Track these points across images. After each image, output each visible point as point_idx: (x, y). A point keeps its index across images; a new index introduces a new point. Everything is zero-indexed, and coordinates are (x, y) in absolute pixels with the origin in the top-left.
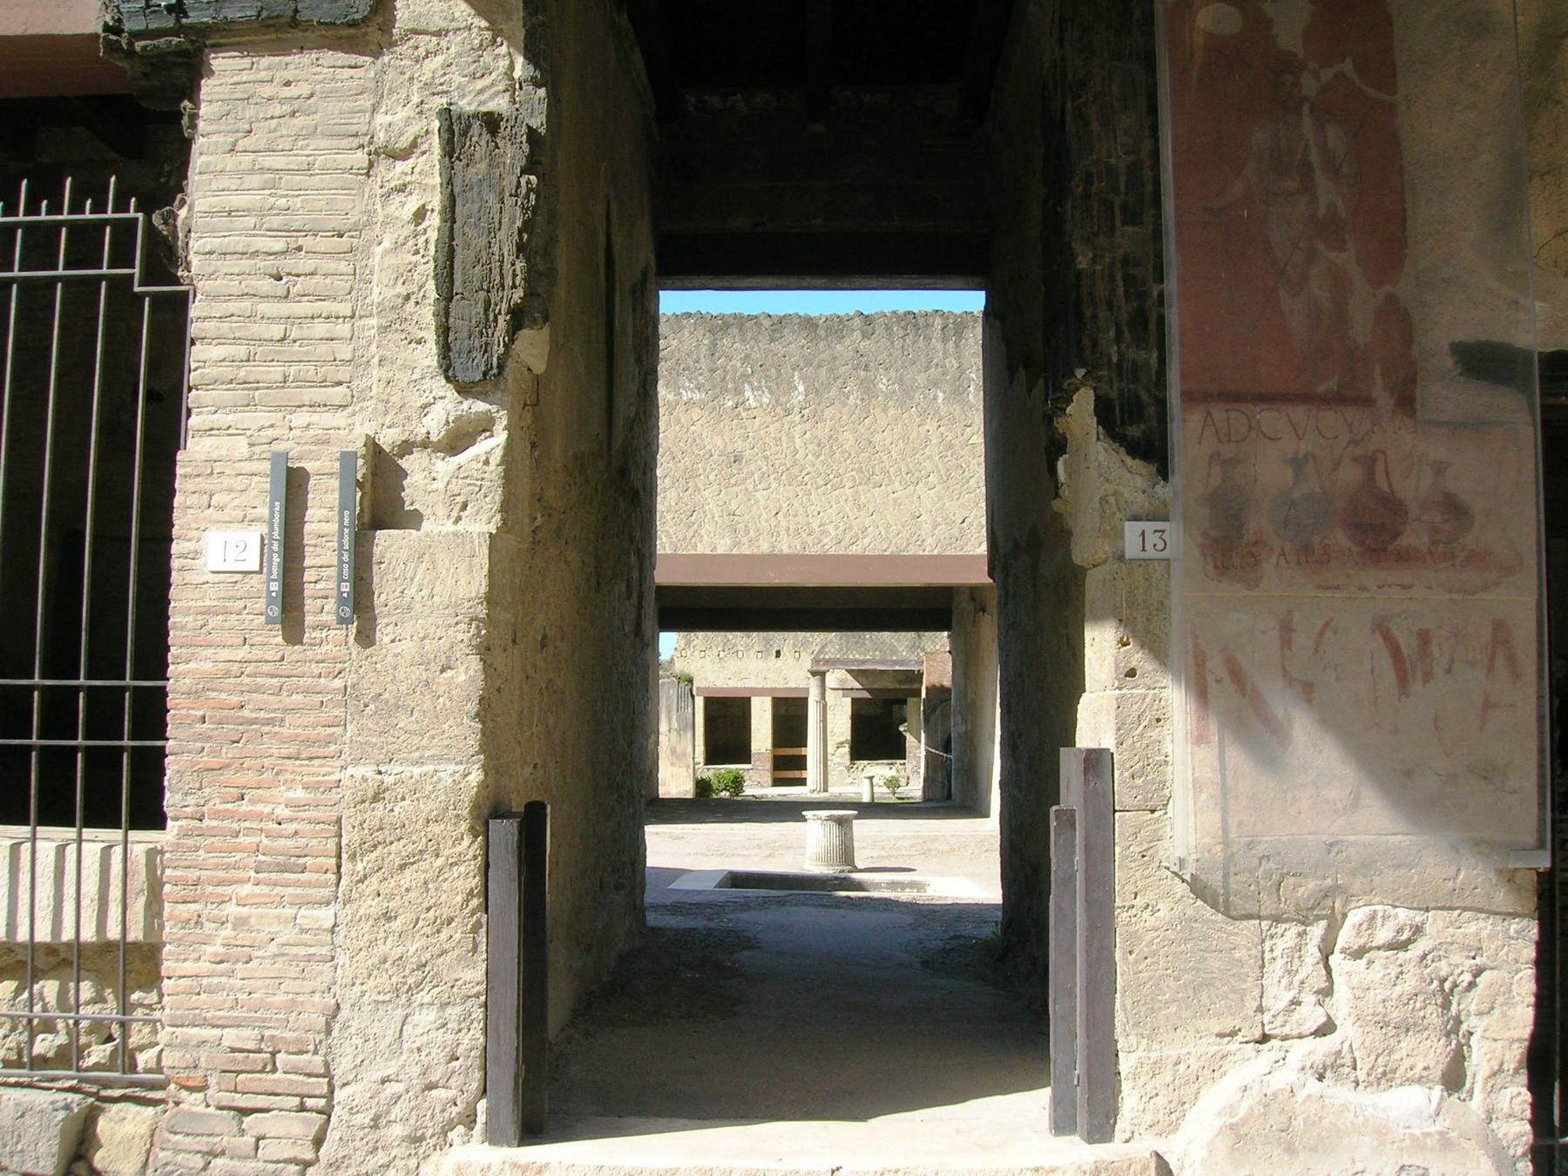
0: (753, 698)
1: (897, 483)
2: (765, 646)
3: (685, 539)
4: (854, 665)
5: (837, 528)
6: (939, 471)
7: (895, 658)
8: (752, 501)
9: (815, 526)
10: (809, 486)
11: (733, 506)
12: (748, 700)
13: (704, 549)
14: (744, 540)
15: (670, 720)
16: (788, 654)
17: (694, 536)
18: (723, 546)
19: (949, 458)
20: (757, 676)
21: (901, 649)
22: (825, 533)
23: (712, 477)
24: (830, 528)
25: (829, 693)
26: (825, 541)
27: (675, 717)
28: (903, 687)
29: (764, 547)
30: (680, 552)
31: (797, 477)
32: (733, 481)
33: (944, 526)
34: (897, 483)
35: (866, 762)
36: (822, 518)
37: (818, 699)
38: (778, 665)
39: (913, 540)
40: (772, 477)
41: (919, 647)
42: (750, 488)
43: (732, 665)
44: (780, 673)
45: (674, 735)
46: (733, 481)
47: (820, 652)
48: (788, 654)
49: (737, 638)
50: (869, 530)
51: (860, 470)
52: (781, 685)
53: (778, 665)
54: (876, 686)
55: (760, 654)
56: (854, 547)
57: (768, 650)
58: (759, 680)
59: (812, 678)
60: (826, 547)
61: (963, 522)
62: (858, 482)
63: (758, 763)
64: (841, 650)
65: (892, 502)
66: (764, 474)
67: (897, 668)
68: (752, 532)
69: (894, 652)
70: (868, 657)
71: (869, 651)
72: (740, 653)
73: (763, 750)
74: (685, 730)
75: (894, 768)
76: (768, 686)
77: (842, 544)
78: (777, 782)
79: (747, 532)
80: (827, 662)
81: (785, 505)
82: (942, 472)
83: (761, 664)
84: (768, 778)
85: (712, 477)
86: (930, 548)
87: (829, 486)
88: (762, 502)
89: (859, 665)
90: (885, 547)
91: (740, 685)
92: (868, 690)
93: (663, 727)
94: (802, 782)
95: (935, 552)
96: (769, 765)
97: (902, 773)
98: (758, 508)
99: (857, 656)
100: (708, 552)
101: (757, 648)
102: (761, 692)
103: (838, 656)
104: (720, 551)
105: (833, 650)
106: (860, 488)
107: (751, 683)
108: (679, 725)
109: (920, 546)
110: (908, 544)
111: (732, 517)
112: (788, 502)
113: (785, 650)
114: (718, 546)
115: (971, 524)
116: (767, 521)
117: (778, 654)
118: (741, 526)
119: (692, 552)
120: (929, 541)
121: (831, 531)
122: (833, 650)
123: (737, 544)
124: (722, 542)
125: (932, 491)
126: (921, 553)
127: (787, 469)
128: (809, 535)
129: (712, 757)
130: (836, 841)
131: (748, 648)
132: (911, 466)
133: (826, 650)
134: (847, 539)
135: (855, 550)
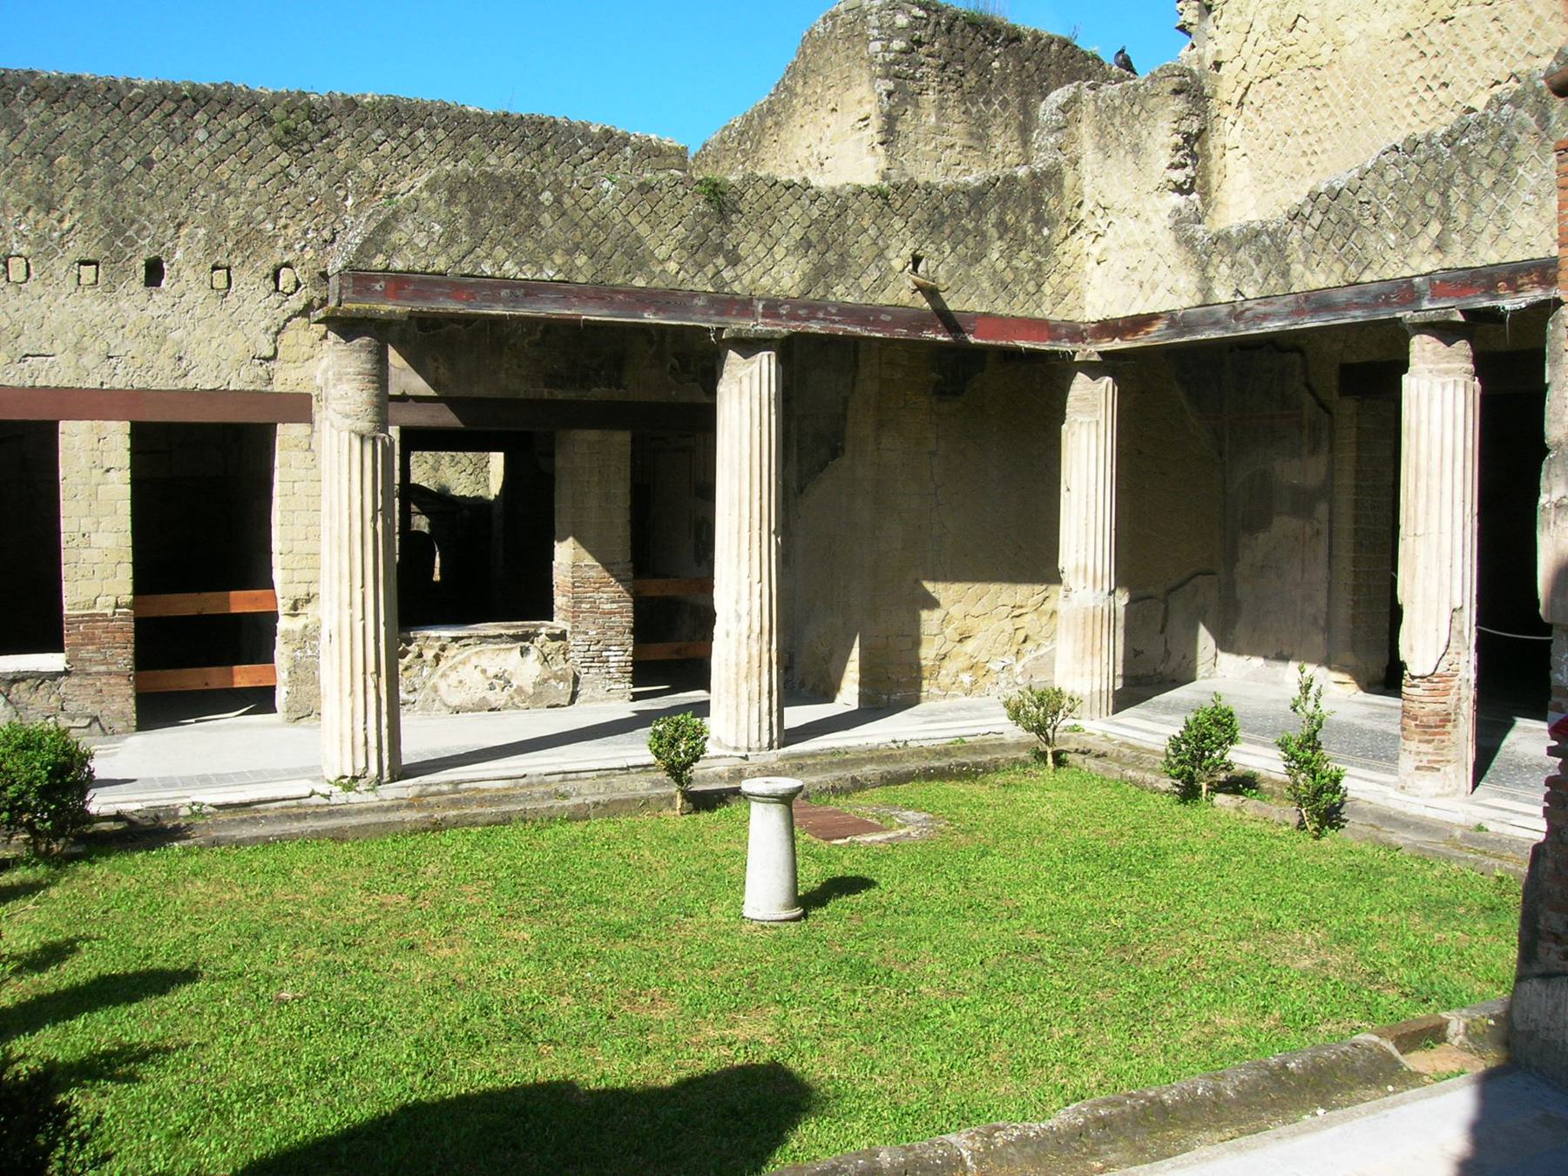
0: (63, 426)
4: (496, 299)
7: (640, 282)
12: (56, 423)
16: (188, 274)
20: (79, 349)
21: (661, 252)
28: (560, 395)
35: (446, 633)
37: (365, 425)
38: (152, 310)
41: (719, 248)
44: (162, 339)
47: (371, 244)
48: (188, 274)
52: (162, 379)
53: (152, 310)
54: (479, 391)
55: (88, 273)
57: (118, 257)
58: (89, 360)
64: (452, 240)
67: (649, 318)
69: (638, 258)
70: (549, 273)
71: (550, 250)
73: (104, 607)
75: (534, 653)
76: (119, 383)
83: (94, 308)
89: (514, 301)
92: (453, 403)
96: (124, 658)
97: (559, 666)
99: (510, 269)
101: (78, 247)
102: (94, 404)
103: (441, 264)
105: (421, 240)
107: (58, 373)
113: (182, 261)
117: (154, 273)
122: (421, 240)
131: (46, 247)
133: (394, 237)
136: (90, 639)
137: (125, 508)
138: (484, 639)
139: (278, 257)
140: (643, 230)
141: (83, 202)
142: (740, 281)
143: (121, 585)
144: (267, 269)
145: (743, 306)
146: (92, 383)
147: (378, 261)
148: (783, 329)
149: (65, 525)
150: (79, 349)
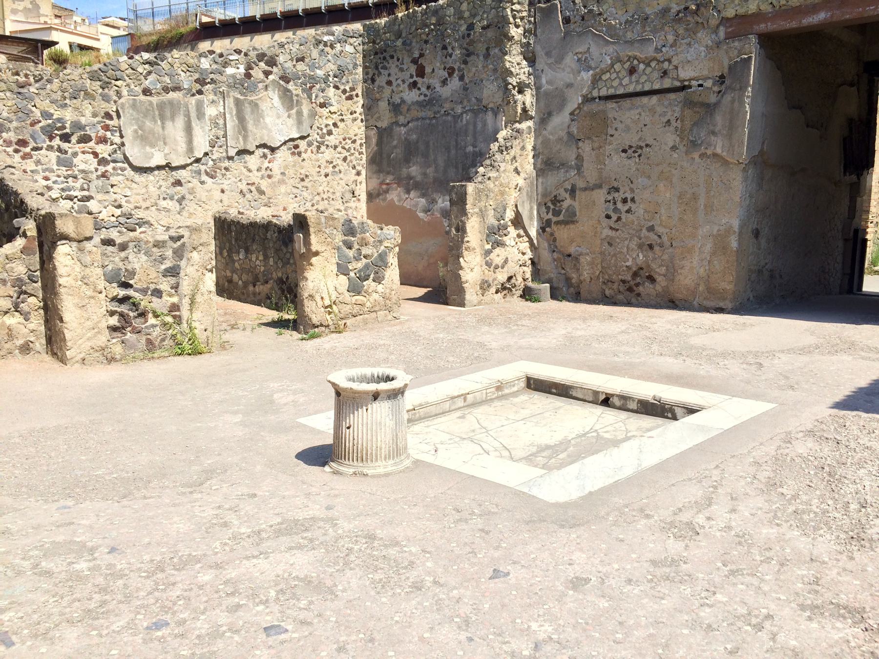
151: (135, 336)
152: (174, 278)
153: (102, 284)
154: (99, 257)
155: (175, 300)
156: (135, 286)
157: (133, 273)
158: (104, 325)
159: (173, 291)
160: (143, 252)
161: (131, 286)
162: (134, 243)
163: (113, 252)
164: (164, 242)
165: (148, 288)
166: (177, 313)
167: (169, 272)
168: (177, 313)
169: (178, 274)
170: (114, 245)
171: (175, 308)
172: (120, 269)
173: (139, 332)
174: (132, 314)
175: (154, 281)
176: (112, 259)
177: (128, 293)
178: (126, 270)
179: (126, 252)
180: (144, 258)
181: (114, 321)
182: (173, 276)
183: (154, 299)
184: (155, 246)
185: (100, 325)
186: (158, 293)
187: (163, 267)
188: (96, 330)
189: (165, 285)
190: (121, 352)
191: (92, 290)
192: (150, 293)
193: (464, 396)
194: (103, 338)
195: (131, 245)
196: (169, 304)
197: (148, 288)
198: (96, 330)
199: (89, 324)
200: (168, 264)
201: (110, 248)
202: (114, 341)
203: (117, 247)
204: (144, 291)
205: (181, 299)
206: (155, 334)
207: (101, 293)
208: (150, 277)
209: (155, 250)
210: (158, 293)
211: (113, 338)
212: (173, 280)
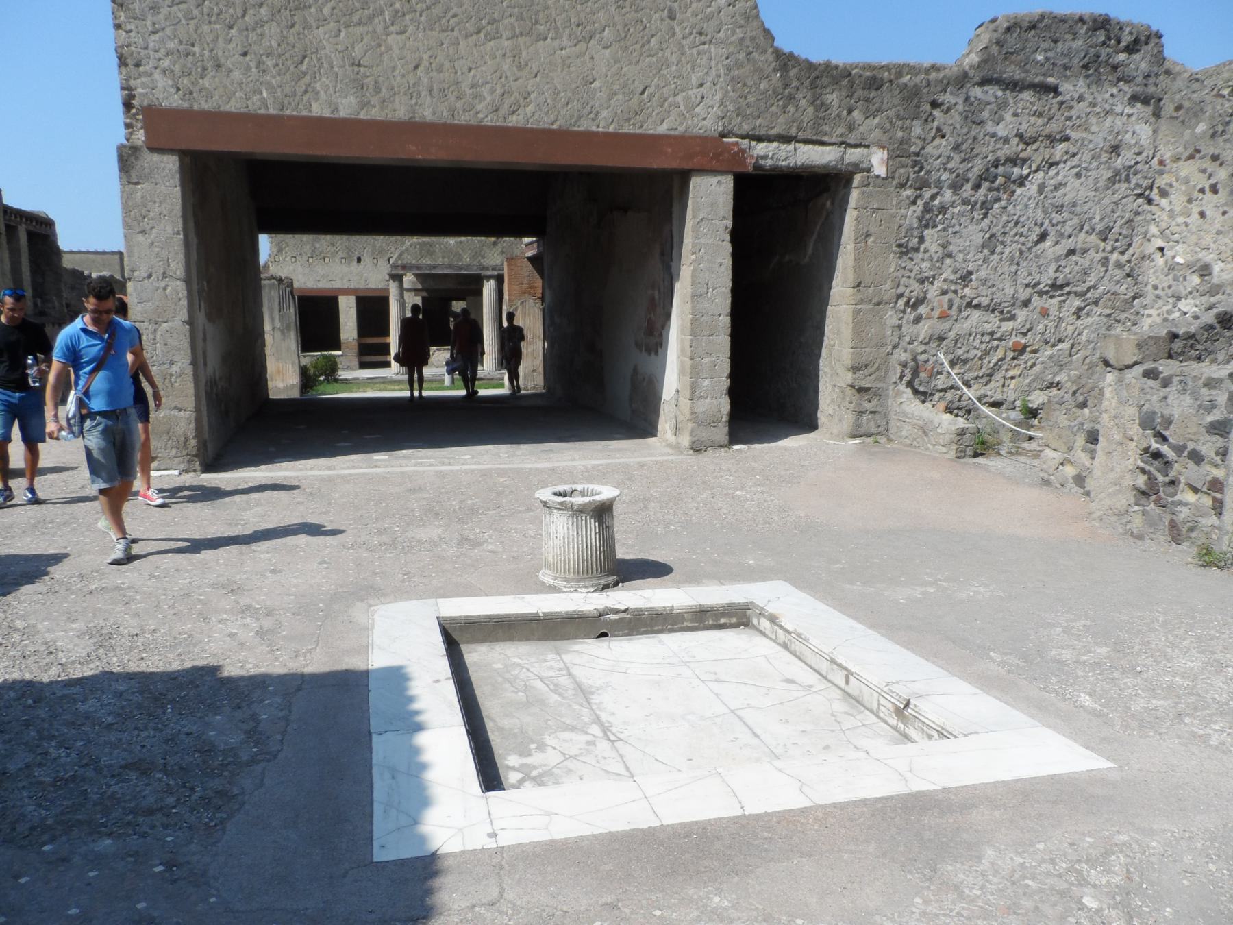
0: (340, 297)
1: (565, 37)
2: (348, 253)
3: (294, 94)
5: (492, 91)
6: (615, 25)
8: (383, 48)
9: (465, 86)
10: (456, 33)
11: (358, 51)
13: (318, 109)
14: (374, 101)
15: (272, 320)
17: (306, 92)
18: (347, 107)
19: (628, 9)
20: (342, 279)
22: (480, 97)
23: (326, 11)
24: (485, 90)
25: (406, 294)
26: (480, 107)
27: (277, 317)
29: (400, 111)
30: (288, 112)
31: (440, 19)
32: (356, 18)
33: (621, 96)
34: (565, 37)
36: (474, 76)
39: (585, 112)
40: (408, 17)
42: (380, 29)
43: (321, 269)
44: (362, 276)
45: (278, 334)
46: (356, 18)
49: (325, 242)
50: (533, 96)
51: (520, 18)
52: (362, 286)
55: (343, 260)
56: (515, 117)
57: (350, 256)
58: (345, 281)
59: (391, 282)
60: (480, 116)
61: (643, 92)
62: (517, 31)
63: (347, 350)
65: (559, 61)
66: (397, 12)
67: (463, 272)
68: (384, 90)
72: (327, 259)
74: (288, 328)
76: (352, 287)
77: (501, 113)
78: (363, 365)
79: (377, 90)
80: (404, 267)
81: (426, 57)
82: (620, 27)
83: (345, 269)
84: (355, 362)
85: (326, 11)
86: (604, 123)
87: (482, 35)
88: (396, 52)
90: (552, 118)
91: (328, 285)
93: (267, 327)
94: (387, 365)
95: (611, 129)
96: (355, 351)
98: (391, 59)
100: (327, 114)
101: (340, 254)
102: (346, 292)
103: (414, 262)
104: (343, 114)
106: (521, 40)
107: (337, 284)
108: (282, 325)
109: (593, 120)
110: (580, 117)
111: (356, 68)
112: (430, 53)
114: (341, 107)
115: (652, 95)
116: (403, 76)
117: (359, 260)
118: (369, 81)
119: (305, 113)
120: (604, 114)
121: (485, 94)
123: (365, 104)
124: (344, 101)
125: (608, 51)
126: (594, 129)
127: (428, 8)
128: (458, 98)
129: (307, 345)
130: (594, 540)
132: (582, 16)
134: (506, 106)
135: (514, 121)
136: (348, 348)
137: (355, 316)
138: (445, 350)
139: (389, 255)
140: (461, 252)
141: (341, 244)
142: (485, 262)
143: (354, 334)
144: (386, 258)
145: (487, 268)
146: (346, 287)
147: (400, 262)
148: (496, 273)
149: (341, 320)
150: (342, 279)
151: (1158, 510)
152: (1222, 439)
153: (1135, 430)
154: (1136, 393)
155: (1219, 473)
156: (1171, 440)
157: (1168, 422)
158: (1128, 481)
159: (1218, 458)
160: (1189, 392)
161: (1165, 439)
162: (1178, 378)
163: (1152, 388)
164: (1220, 381)
165: (1185, 447)
166: (1218, 496)
167: (1215, 428)
168: (1218, 496)
169: (1228, 433)
170: (1155, 378)
171: (1216, 485)
172: (1154, 413)
173: (1164, 507)
174: (1161, 478)
175: (1193, 437)
176: (1149, 397)
177: (1158, 446)
178: (1162, 416)
179: (1167, 389)
180: (1188, 400)
181: (1141, 481)
182: (1221, 436)
183: (1191, 465)
184: (1205, 385)
185: (1122, 481)
186: (1196, 457)
187: (1209, 419)
188: (1118, 487)
189: (1208, 446)
190: (1140, 526)
191: (1121, 434)
192: (1186, 453)
193: (848, 674)
194: (1125, 499)
195: (1175, 379)
196: (1209, 478)
197: (1185, 447)
198: (1118, 487)
199: (1112, 476)
200: (1216, 416)
201: (1151, 382)
202: (1137, 508)
203: (1159, 381)
204: (1179, 450)
205: (1227, 475)
206: (1182, 516)
207: (1132, 440)
208: (1189, 430)
209: (1204, 391)
210: (1196, 457)
211: (1136, 504)
212: (1219, 442)
